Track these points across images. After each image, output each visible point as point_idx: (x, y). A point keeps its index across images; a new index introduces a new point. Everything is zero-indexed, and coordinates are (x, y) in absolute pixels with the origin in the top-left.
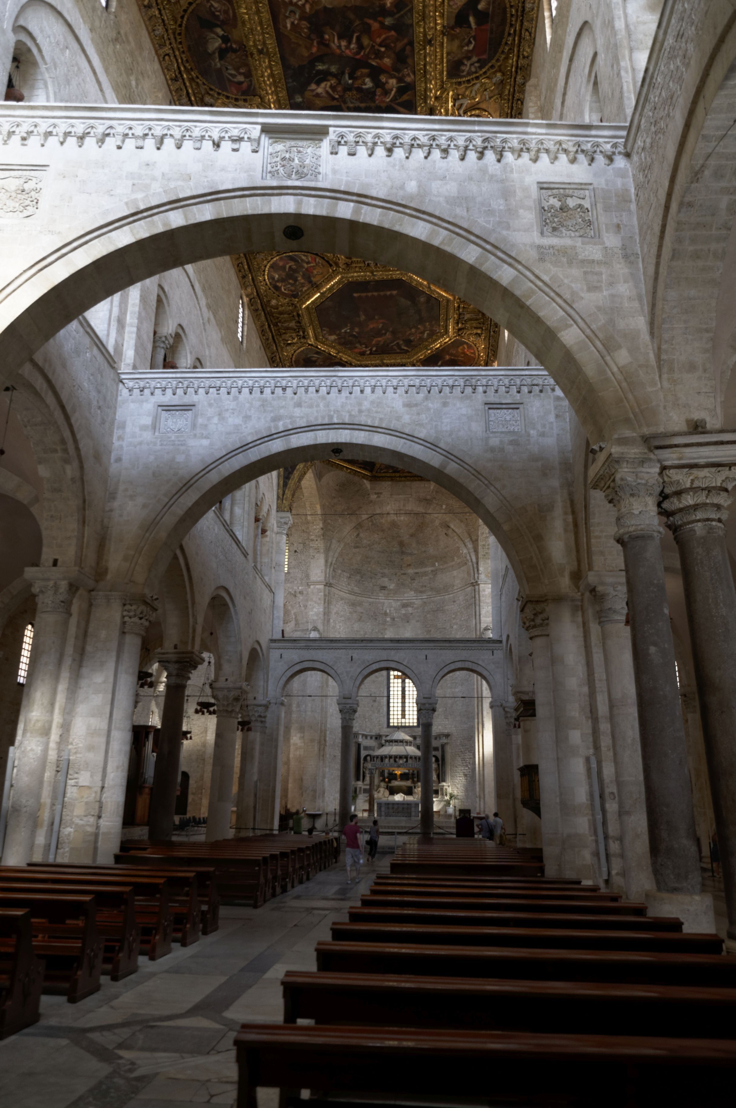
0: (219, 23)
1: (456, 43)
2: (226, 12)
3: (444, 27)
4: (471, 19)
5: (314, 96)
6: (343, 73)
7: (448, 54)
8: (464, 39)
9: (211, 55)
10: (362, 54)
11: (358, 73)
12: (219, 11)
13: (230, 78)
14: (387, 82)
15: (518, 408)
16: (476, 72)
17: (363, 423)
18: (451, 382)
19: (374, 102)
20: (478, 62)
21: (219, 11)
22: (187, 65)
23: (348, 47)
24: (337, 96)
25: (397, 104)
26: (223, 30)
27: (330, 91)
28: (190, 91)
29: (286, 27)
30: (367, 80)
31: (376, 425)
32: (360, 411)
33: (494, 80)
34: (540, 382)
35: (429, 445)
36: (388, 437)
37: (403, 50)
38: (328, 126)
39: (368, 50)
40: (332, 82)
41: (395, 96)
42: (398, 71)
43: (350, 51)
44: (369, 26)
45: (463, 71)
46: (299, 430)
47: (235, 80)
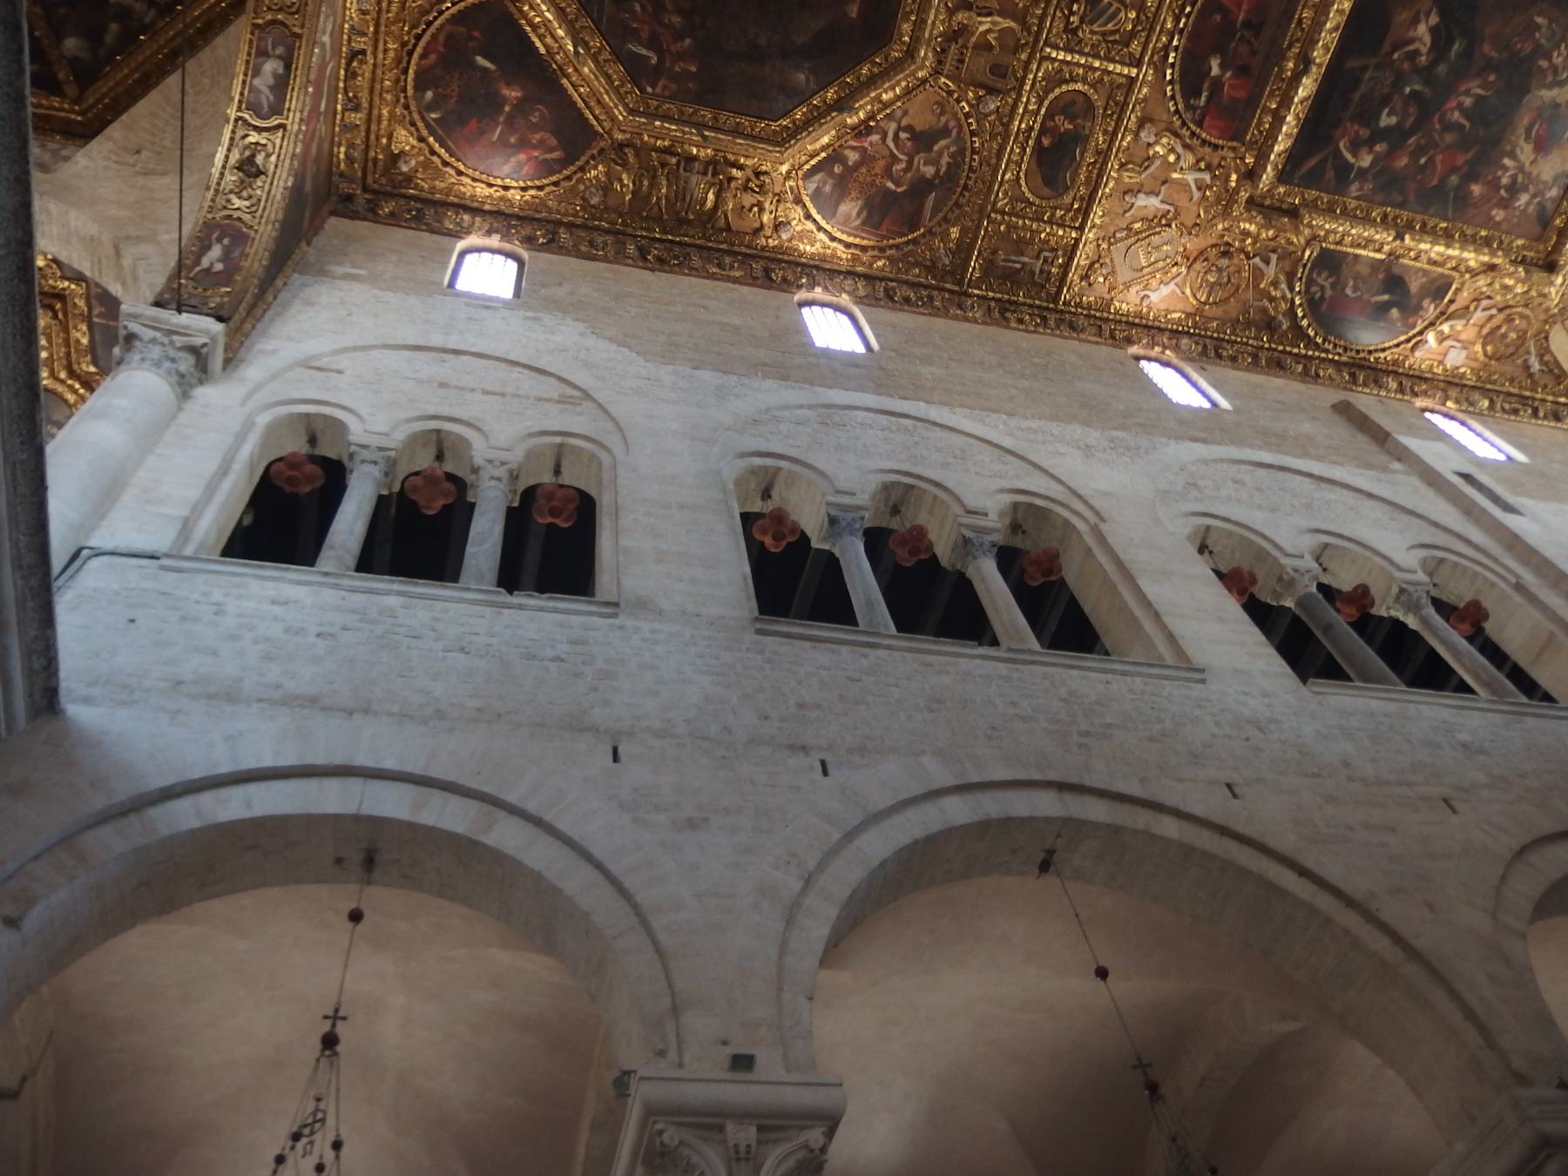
1: (1364, 270)
3: (1398, 257)
4: (1386, 297)
5: (1418, 13)
6: (1427, 83)
7: (1357, 256)
11: (1412, 110)
14: (1371, 151)
20: (1322, 298)
23: (1460, 106)
24: (1396, 56)
27: (1411, 47)
29: (1539, 15)
30: (1394, 120)
33: (1280, 317)
39: (1437, 137)
40: (1423, 58)
41: (1342, 156)
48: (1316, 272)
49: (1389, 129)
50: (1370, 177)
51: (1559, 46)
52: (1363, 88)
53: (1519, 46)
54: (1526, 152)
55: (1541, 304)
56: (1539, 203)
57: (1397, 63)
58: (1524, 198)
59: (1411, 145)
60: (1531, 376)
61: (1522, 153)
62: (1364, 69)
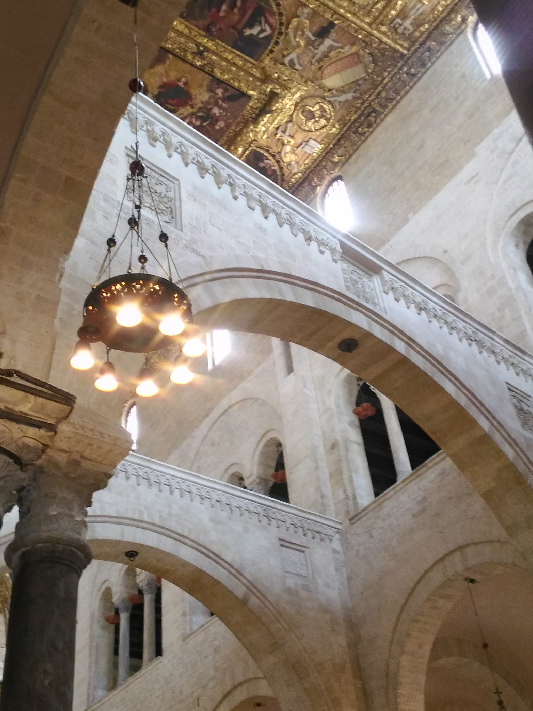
15: (303, 552)
17: (173, 529)
18: (252, 509)
31: (185, 534)
32: (170, 515)
34: (323, 531)
35: (233, 571)
36: (195, 552)
38: (381, 268)
46: (107, 519)
58: (216, 111)
60: (355, 98)
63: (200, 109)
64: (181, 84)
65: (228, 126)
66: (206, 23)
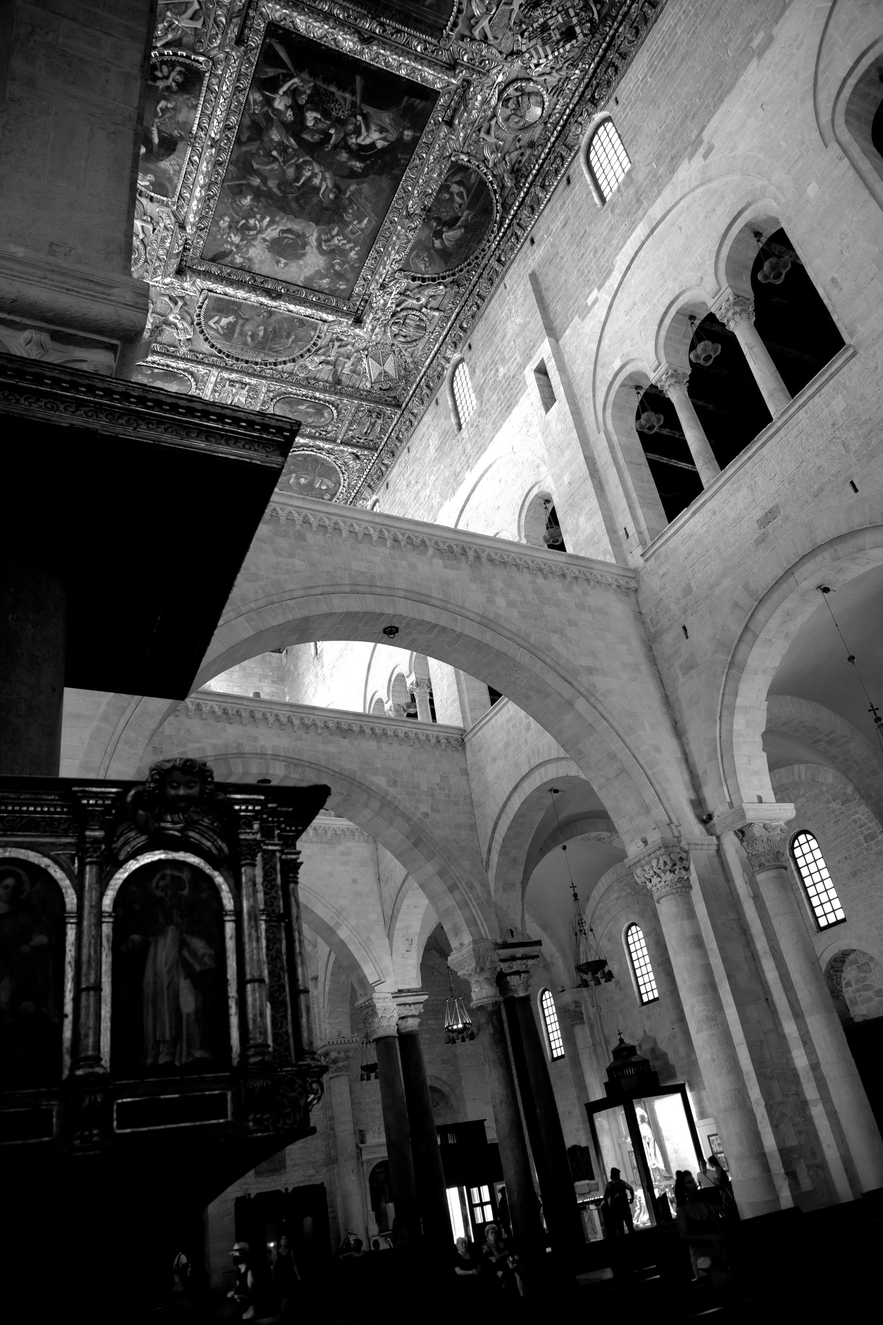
0: (432, 251)
1: (181, 117)
2: (418, 256)
4: (156, 140)
5: (387, 131)
6: (335, 146)
7: (195, 107)
8: (169, 118)
9: (465, 226)
10: (301, 160)
11: (317, 137)
12: (423, 259)
13: (465, 195)
14: (287, 107)
16: (163, 62)
19: (315, 86)
20: (156, 79)
21: (423, 259)
22: (495, 229)
23: (314, 175)
24: (359, 118)
25: (288, 69)
26: (433, 243)
27: (363, 130)
28: (517, 203)
30: (310, 123)
37: (250, 140)
39: (293, 161)
40: (354, 141)
41: (285, 82)
42: (266, 115)
43: (313, 168)
44: (279, 186)
45: (180, 73)
47: (462, 189)
48: (183, 70)
49: (303, 119)
50: (266, 109)
51: (345, 239)
52: (339, 94)
53: (350, 211)
54: (272, 233)
55: (147, 271)
56: (231, 251)
57: (354, 120)
58: (236, 239)
59: (288, 140)
61: (272, 230)
62: (353, 93)
63: (254, 238)
64: (283, 261)
65: (216, 223)
66: (273, 318)
